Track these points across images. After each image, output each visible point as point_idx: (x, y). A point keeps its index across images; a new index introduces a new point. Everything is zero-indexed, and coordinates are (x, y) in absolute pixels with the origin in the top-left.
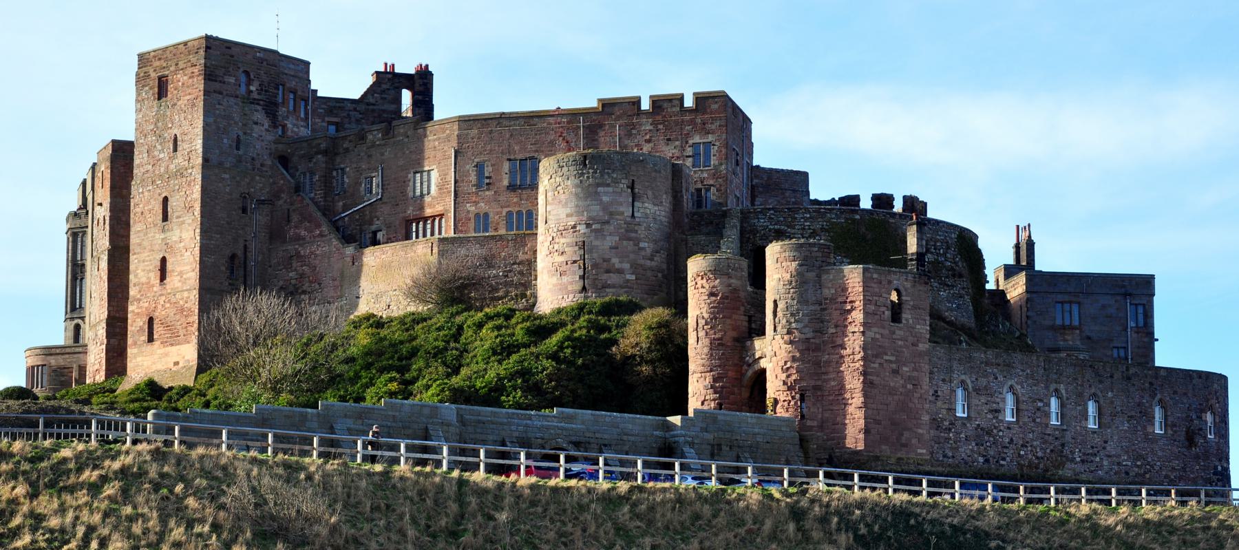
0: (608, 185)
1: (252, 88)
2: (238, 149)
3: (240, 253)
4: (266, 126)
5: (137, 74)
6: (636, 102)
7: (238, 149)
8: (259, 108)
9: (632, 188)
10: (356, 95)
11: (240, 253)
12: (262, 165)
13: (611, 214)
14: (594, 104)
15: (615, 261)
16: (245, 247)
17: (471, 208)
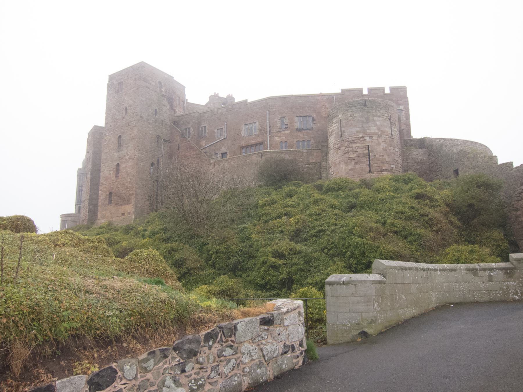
0: (379, 116)
1: (162, 90)
2: (156, 115)
3: (156, 163)
4: (168, 108)
5: (108, 84)
6: (361, 90)
7: (156, 115)
8: (165, 99)
9: (390, 120)
10: (204, 104)
11: (156, 163)
12: (166, 124)
13: (382, 131)
14: (340, 92)
15: (386, 157)
16: (158, 160)
17: (277, 139)
